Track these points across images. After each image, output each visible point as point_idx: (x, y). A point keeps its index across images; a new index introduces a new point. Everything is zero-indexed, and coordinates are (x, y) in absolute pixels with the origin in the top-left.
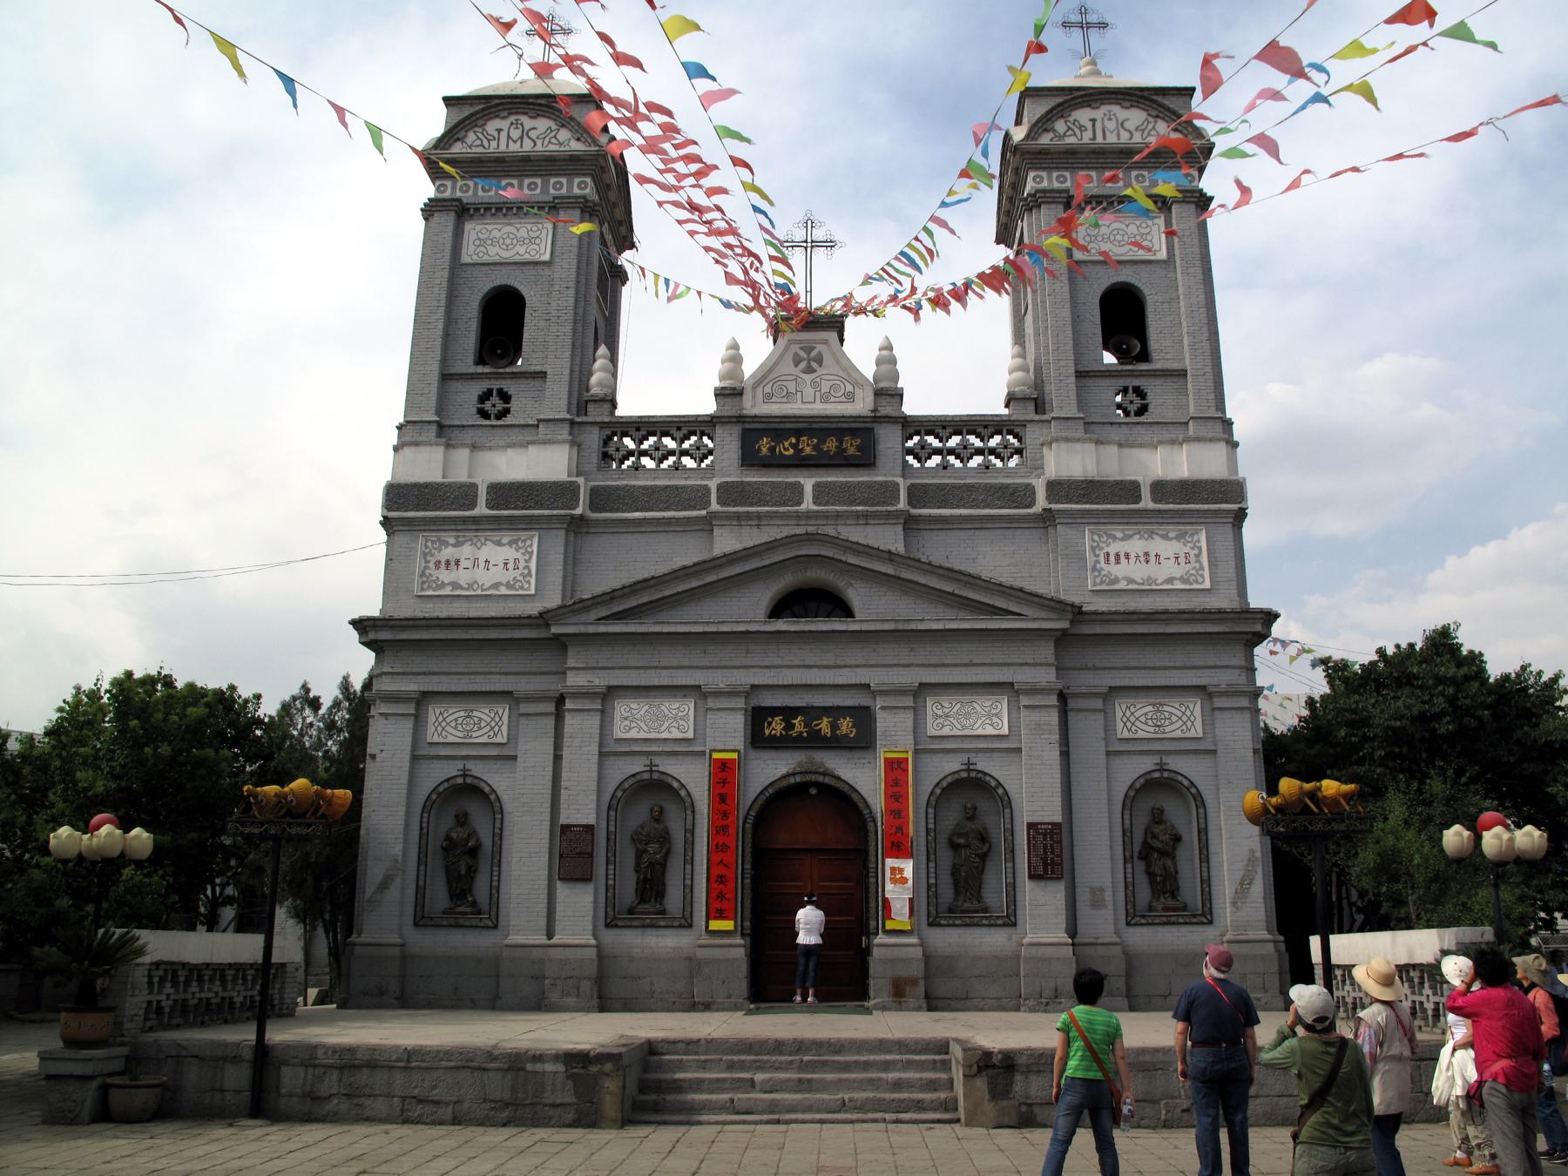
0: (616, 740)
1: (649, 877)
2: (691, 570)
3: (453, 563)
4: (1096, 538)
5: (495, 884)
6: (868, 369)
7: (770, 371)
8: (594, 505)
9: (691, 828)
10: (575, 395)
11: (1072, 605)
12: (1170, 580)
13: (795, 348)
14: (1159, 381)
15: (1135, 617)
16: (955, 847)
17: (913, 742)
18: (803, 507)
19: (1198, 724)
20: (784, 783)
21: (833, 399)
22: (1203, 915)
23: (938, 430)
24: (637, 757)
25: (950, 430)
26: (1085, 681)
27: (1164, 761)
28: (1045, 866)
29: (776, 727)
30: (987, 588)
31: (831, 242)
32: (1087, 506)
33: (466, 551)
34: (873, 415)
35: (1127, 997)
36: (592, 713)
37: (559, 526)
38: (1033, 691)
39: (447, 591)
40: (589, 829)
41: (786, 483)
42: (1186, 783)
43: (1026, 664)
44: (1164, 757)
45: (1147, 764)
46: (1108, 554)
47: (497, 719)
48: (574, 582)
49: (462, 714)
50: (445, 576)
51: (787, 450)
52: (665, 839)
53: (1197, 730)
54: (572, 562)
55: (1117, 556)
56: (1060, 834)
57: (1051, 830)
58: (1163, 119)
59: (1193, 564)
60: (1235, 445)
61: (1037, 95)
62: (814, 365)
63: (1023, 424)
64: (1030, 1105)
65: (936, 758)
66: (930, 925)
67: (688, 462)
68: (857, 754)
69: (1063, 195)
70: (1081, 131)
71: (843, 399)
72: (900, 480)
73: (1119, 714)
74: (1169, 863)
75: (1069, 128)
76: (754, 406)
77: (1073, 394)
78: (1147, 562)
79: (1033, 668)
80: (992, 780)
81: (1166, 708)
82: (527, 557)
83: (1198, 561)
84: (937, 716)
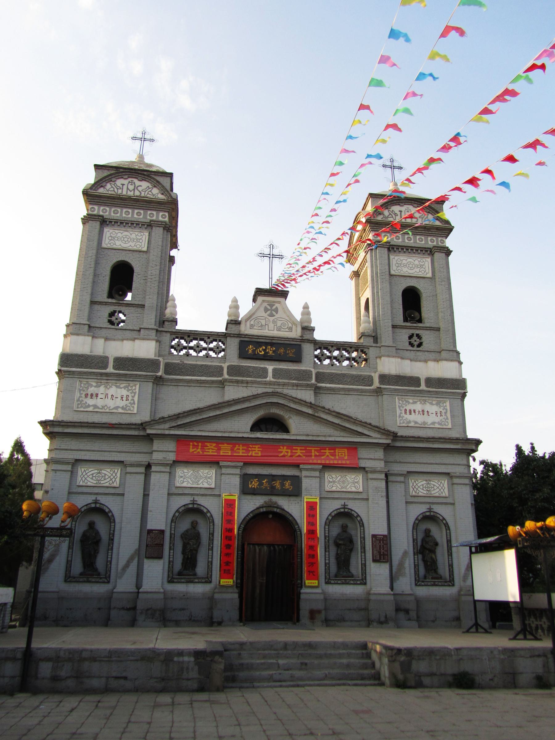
0: (411, 496)
1: (190, 557)
2: (217, 406)
3: (94, 395)
4: (401, 402)
5: (109, 559)
6: (298, 316)
7: (254, 314)
8: (166, 372)
9: (212, 532)
10: (158, 318)
11: (393, 433)
12: (433, 423)
13: (265, 304)
14: (428, 332)
15: (419, 439)
16: (337, 545)
17: (319, 493)
18: (268, 379)
19: (446, 490)
20: (257, 512)
21: (282, 330)
22: (450, 581)
23: (330, 348)
24: (186, 496)
25: (335, 348)
26: (396, 468)
27: (431, 507)
28: (380, 555)
29: (254, 484)
30: (355, 423)
31: (281, 256)
32: (397, 387)
33: (102, 390)
34: (301, 338)
35: (417, 621)
36: (165, 474)
37: (150, 381)
38: (374, 471)
39: (91, 409)
40: (162, 532)
41: (260, 367)
42: (441, 518)
43: (371, 459)
44: (431, 505)
45: (423, 509)
46: (406, 410)
47: (114, 475)
48: (155, 408)
49: (96, 471)
50: (90, 402)
51: (261, 352)
52: (197, 537)
53: (446, 493)
54: (155, 399)
55: (410, 411)
56: (387, 540)
57: (383, 538)
58: (431, 214)
59: (444, 416)
60: (461, 363)
61: (375, 197)
62: (274, 313)
63: (368, 347)
64: (420, 676)
65: (330, 501)
66: (326, 583)
67: (212, 354)
68: (292, 499)
69: (388, 244)
70: (395, 216)
71: (287, 330)
72: (312, 370)
73: (411, 485)
74: (434, 556)
75: (390, 214)
76: (245, 329)
77: (391, 337)
78: (423, 414)
79: (374, 461)
80: (355, 513)
81: (432, 482)
82: (133, 395)
83: (446, 415)
84: (330, 482)
